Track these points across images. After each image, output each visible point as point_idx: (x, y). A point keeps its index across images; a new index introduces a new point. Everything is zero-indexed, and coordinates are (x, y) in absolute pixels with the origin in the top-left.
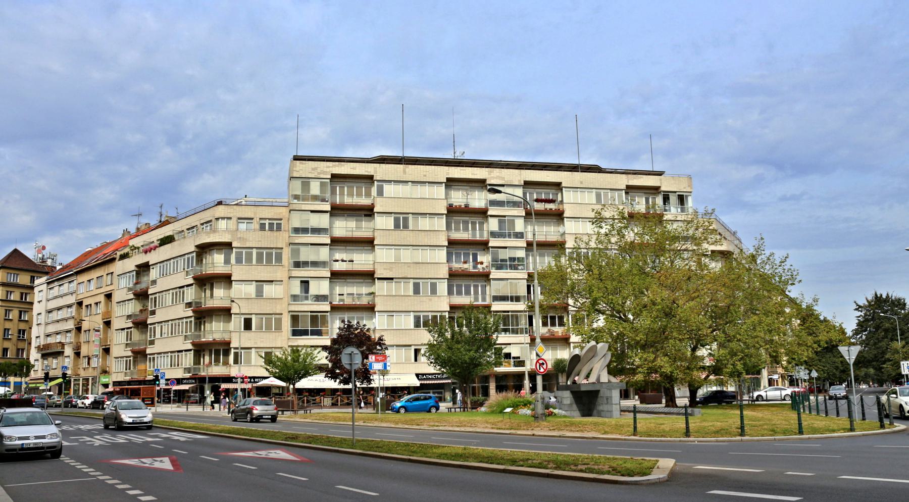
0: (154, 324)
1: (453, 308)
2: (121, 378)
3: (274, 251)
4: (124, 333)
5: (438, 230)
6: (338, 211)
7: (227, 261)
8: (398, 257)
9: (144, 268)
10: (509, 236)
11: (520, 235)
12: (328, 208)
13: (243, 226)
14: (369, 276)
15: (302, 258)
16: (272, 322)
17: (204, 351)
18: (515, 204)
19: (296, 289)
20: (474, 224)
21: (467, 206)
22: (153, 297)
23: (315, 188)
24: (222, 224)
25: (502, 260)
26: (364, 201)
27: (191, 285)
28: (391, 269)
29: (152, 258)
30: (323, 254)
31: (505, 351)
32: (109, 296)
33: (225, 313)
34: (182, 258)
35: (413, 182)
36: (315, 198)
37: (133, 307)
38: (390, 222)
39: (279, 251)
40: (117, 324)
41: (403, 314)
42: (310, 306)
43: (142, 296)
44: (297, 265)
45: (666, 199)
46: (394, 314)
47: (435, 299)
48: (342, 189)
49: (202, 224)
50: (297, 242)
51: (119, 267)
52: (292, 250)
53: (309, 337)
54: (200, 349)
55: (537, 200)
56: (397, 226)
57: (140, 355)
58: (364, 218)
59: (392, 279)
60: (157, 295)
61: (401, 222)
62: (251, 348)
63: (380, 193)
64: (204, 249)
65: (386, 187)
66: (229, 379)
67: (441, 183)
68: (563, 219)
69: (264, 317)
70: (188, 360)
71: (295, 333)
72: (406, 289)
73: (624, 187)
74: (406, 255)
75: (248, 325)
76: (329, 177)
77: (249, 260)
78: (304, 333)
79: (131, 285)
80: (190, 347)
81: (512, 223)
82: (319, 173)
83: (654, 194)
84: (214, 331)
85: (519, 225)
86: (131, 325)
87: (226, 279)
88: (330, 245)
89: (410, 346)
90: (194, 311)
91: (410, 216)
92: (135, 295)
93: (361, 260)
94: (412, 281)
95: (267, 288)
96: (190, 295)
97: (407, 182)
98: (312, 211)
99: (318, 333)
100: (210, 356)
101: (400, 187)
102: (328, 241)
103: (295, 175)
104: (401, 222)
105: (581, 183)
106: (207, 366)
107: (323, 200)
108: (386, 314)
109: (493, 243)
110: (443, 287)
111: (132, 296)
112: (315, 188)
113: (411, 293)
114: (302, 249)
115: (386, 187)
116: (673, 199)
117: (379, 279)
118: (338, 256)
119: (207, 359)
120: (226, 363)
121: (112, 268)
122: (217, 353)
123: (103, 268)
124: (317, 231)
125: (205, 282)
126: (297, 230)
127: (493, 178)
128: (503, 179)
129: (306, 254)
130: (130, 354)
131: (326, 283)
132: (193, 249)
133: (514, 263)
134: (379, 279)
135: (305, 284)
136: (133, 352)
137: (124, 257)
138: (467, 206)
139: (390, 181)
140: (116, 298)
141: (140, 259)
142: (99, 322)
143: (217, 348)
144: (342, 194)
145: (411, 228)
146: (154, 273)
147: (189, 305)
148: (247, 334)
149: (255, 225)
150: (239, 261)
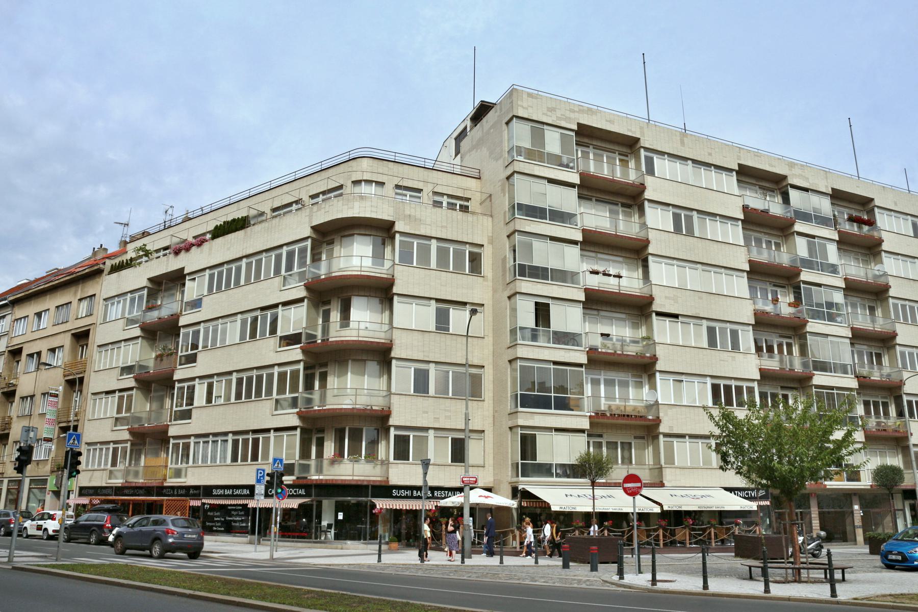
0: (193, 379)
1: (766, 376)
2: (100, 480)
4: (114, 400)
5: (733, 245)
7: (378, 256)
11: (833, 269)
17: (322, 431)
18: (823, 221)
19: (527, 317)
22: (191, 330)
23: (553, 143)
27: (301, 300)
29: (190, 261)
32: (81, 337)
33: (380, 355)
34: (273, 255)
35: (695, 161)
40: (95, 383)
42: (546, 351)
43: (161, 332)
46: (683, 378)
49: (313, 197)
50: (528, 229)
51: (109, 285)
53: (553, 411)
54: (315, 428)
55: (851, 219)
57: (148, 439)
59: (676, 316)
60: (202, 327)
61: (683, 219)
62: (426, 429)
63: (651, 171)
64: (329, 234)
65: (657, 161)
66: (385, 490)
67: (731, 170)
68: (879, 253)
69: (451, 370)
70: (287, 449)
71: (527, 401)
72: (698, 336)
74: (693, 278)
76: (575, 127)
78: (543, 403)
79: (136, 313)
80: (295, 421)
82: (558, 118)
84: (350, 390)
85: (832, 253)
86: (132, 383)
87: (382, 292)
90: (304, 351)
91: (695, 213)
94: (705, 322)
96: (295, 319)
97: (686, 159)
98: (551, 181)
99: (563, 405)
101: (678, 165)
102: (579, 237)
103: (521, 113)
104: (683, 219)
105: (896, 204)
106: (333, 462)
108: (671, 378)
109: (806, 276)
110: (747, 338)
111: (137, 332)
112: (553, 143)
113: (706, 345)
114: (537, 244)
117: (659, 314)
119: (329, 448)
120: (372, 456)
121: (90, 288)
122: (356, 436)
123: (73, 289)
125: (330, 294)
129: (544, 255)
130: (126, 436)
131: (578, 310)
132: (307, 232)
133: (829, 313)
134: (659, 314)
135: (542, 312)
136: (132, 432)
137: (115, 269)
139: (662, 153)
140: (99, 336)
142: (55, 380)
143: (356, 425)
146: (192, 289)
147: (291, 340)
148: (421, 402)
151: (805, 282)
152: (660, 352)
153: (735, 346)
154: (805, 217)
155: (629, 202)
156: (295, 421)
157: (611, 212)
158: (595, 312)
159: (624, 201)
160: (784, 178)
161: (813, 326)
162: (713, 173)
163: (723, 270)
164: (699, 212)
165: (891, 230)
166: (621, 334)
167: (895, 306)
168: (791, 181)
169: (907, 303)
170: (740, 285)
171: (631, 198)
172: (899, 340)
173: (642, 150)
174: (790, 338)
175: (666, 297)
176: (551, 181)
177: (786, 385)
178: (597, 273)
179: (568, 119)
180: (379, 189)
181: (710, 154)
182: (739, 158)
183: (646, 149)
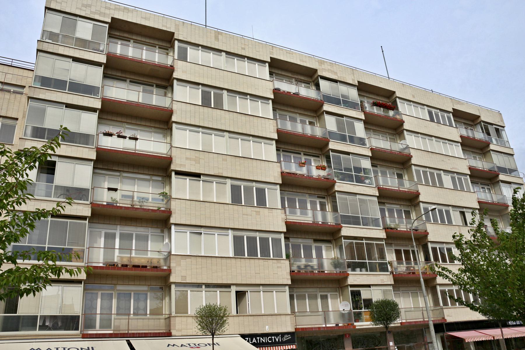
1: (293, 230)
11: (362, 142)
28: (197, 161)
31: (365, 294)
35: (227, 53)
36: (83, 43)
38: (196, 96)
41: (216, 232)
46: (202, 230)
52: (31, 109)
55: (375, 104)
58: (155, 90)
59: (198, 175)
61: (212, 96)
63: (183, 57)
65: (191, 52)
67: (264, 62)
68: (402, 132)
74: (219, 144)
76: (109, 20)
85: (360, 130)
89: (228, 286)
91: (225, 92)
94: (229, 182)
97: (220, 51)
98: (76, 60)
101: (211, 55)
108: (188, 230)
109: (333, 145)
110: (274, 196)
113: (229, 200)
114: (51, 110)
115: (191, 52)
116: (492, 130)
117: (178, 173)
124: (76, 88)
127: (325, 70)
134: (178, 173)
151: (334, 151)
152: (174, 205)
153: (262, 202)
154: (336, 101)
155: (163, 83)
157: (144, 91)
158: (118, 174)
159: (159, 82)
160: (316, 71)
161: (340, 186)
163: (251, 138)
164: (228, 90)
165: (410, 115)
166: (137, 192)
167: (418, 172)
168: (320, 73)
169: (427, 169)
170: (270, 151)
171: (163, 79)
172: (421, 198)
173: (176, 42)
174: (324, 198)
175: (187, 159)
176: (76, 60)
177: (318, 238)
178: (110, 135)
179: (104, 15)
181: (244, 49)
182: (271, 53)
183: (180, 41)
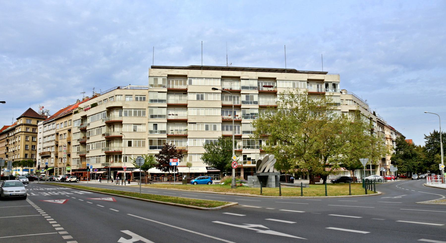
2: (75, 168)
3: (142, 110)
4: (76, 147)
6: (171, 91)
7: (121, 115)
8: (198, 113)
9: (84, 118)
10: (251, 103)
11: (256, 103)
12: (166, 90)
13: (128, 99)
14: (185, 122)
15: (154, 114)
16: (140, 143)
18: (254, 88)
19: (152, 128)
20: (234, 97)
21: (231, 89)
23: (160, 81)
24: (118, 97)
25: (247, 115)
26: (183, 87)
28: (195, 119)
29: (88, 113)
30: (164, 112)
31: (248, 156)
32: (70, 131)
33: (120, 138)
35: (205, 78)
36: (160, 86)
37: (80, 136)
38: (194, 97)
39: (144, 110)
40: (74, 143)
41: (200, 139)
43: (84, 130)
44: (152, 117)
45: (327, 86)
47: (215, 132)
48: (173, 81)
49: (110, 98)
52: (150, 110)
54: (109, 155)
55: (264, 86)
56: (198, 99)
57: (83, 157)
59: (195, 123)
61: (200, 97)
63: (190, 83)
64: (110, 110)
65: (194, 81)
66: (121, 169)
69: (137, 140)
70: (103, 160)
71: (151, 148)
73: (307, 80)
74: (202, 112)
75: (130, 144)
77: (130, 114)
80: (104, 154)
81: (252, 97)
83: (322, 83)
84: (115, 147)
85: (256, 98)
86: (79, 144)
87: (120, 123)
88: (167, 107)
90: (106, 138)
92: (81, 130)
93: (181, 114)
94: (205, 124)
95: (138, 127)
96: (104, 130)
98: (159, 92)
100: (113, 158)
101: (200, 80)
104: (200, 97)
105: (286, 78)
107: (164, 87)
108: (192, 139)
109: (243, 106)
110: (219, 127)
111: (79, 131)
112: (160, 81)
113: (204, 130)
114: (154, 109)
115: (194, 81)
116: (330, 85)
117: (189, 123)
118: (171, 112)
119: (112, 159)
120: (120, 161)
122: (116, 157)
125: (111, 124)
126: (152, 101)
127: (244, 76)
128: (248, 76)
129: (156, 112)
130: (79, 157)
131: (165, 125)
132: (105, 109)
134: (189, 123)
135: (155, 125)
136: (80, 156)
138: (231, 89)
140: (73, 131)
141: (82, 114)
142: (65, 142)
143: (116, 154)
144: (173, 84)
145: (204, 99)
146: (89, 120)
149: (134, 98)
150: (126, 115)
153: (215, 129)
156: (104, 154)
162: (212, 81)
180: (121, 96)
